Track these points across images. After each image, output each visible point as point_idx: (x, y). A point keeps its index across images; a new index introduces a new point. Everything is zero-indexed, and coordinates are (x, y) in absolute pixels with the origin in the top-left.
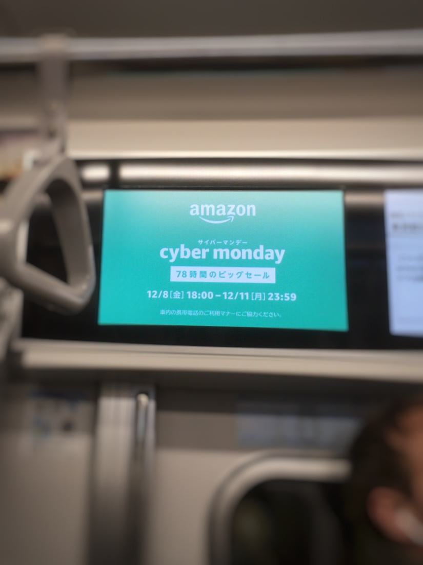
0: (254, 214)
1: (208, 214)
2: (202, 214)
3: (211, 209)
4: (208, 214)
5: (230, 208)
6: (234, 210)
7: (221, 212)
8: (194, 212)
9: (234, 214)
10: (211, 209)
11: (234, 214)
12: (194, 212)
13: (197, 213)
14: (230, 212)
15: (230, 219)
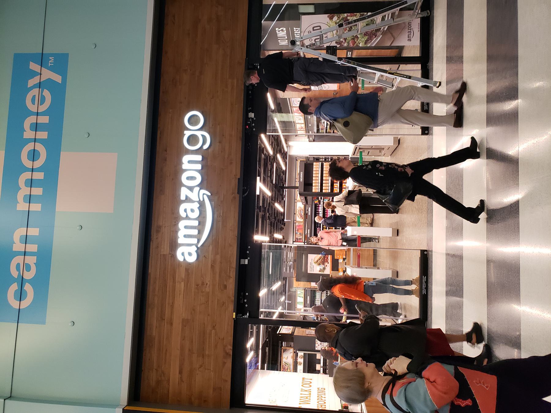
2: (195, 241)
3: (186, 227)
5: (187, 197)
6: (191, 189)
7: (192, 211)
8: (190, 254)
10: (186, 227)
14: (194, 196)
15: (205, 196)
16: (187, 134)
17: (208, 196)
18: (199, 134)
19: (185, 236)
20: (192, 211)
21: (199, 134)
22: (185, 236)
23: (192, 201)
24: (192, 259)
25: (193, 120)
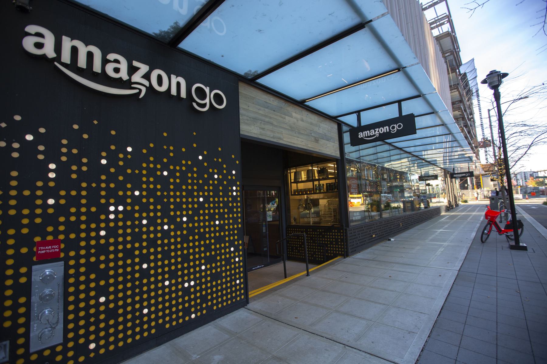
1: (367, 136)
2: (364, 136)
3: (367, 133)
4: (367, 136)
6: (378, 131)
7: (372, 133)
8: (361, 136)
9: (378, 133)
10: (367, 133)
11: (378, 133)
12: (361, 136)
13: (362, 136)
14: (377, 132)
16: (395, 125)
17: (377, 136)
18: (396, 129)
19: (365, 133)
20: (372, 133)
21: (396, 129)
22: (365, 133)
23: (375, 133)
24: (359, 137)
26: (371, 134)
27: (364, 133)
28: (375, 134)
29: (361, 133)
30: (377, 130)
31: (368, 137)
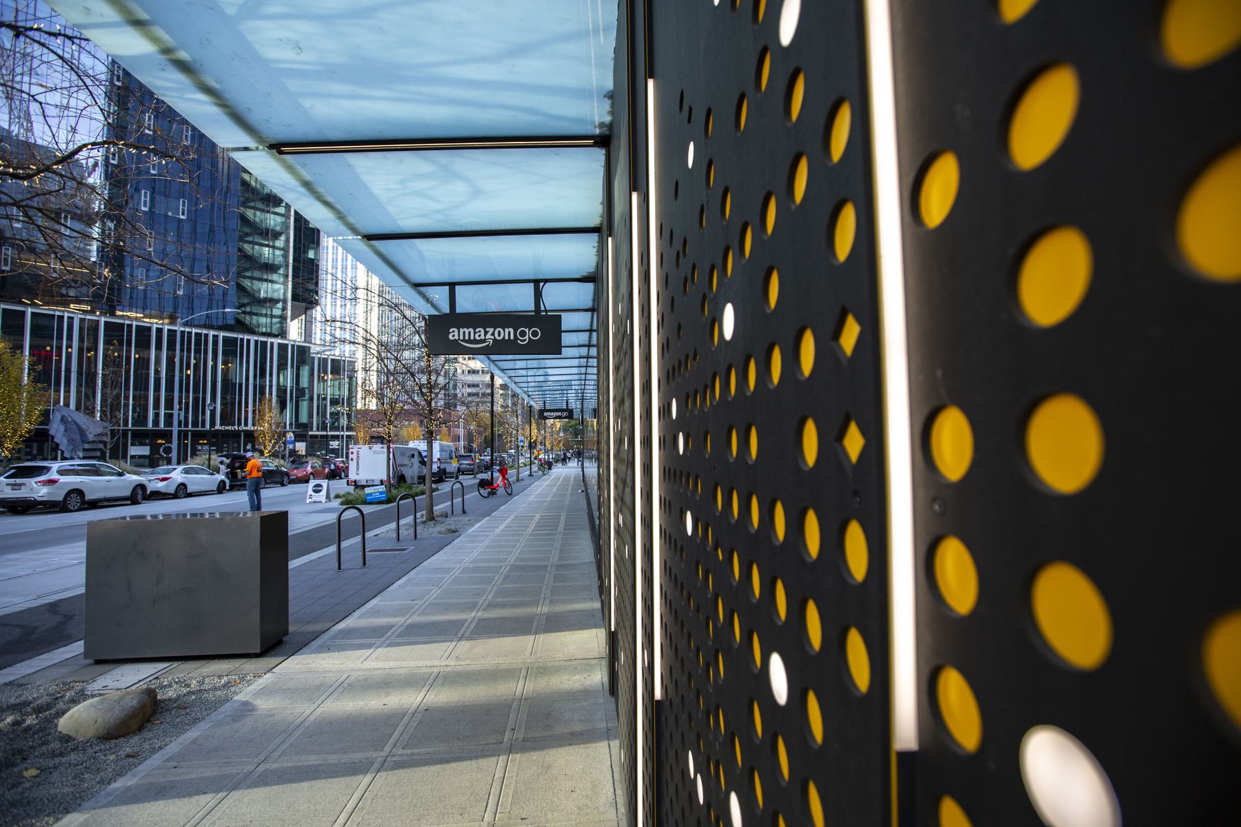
0: (512, 338)
1: (467, 338)
2: (461, 338)
3: (470, 333)
4: (467, 338)
8: (453, 336)
10: (470, 333)
11: (493, 337)
12: (453, 336)
13: (456, 337)
14: (489, 336)
16: (527, 330)
19: (464, 332)
20: (480, 336)
21: (527, 337)
22: (464, 332)
23: (485, 335)
24: (451, 337)
25: (535, 334)
26: (477, 338)
27: (462, 330)
28: (485, 339)
29: (456, 330)
30: (491, 330)
31: (469, 341)
